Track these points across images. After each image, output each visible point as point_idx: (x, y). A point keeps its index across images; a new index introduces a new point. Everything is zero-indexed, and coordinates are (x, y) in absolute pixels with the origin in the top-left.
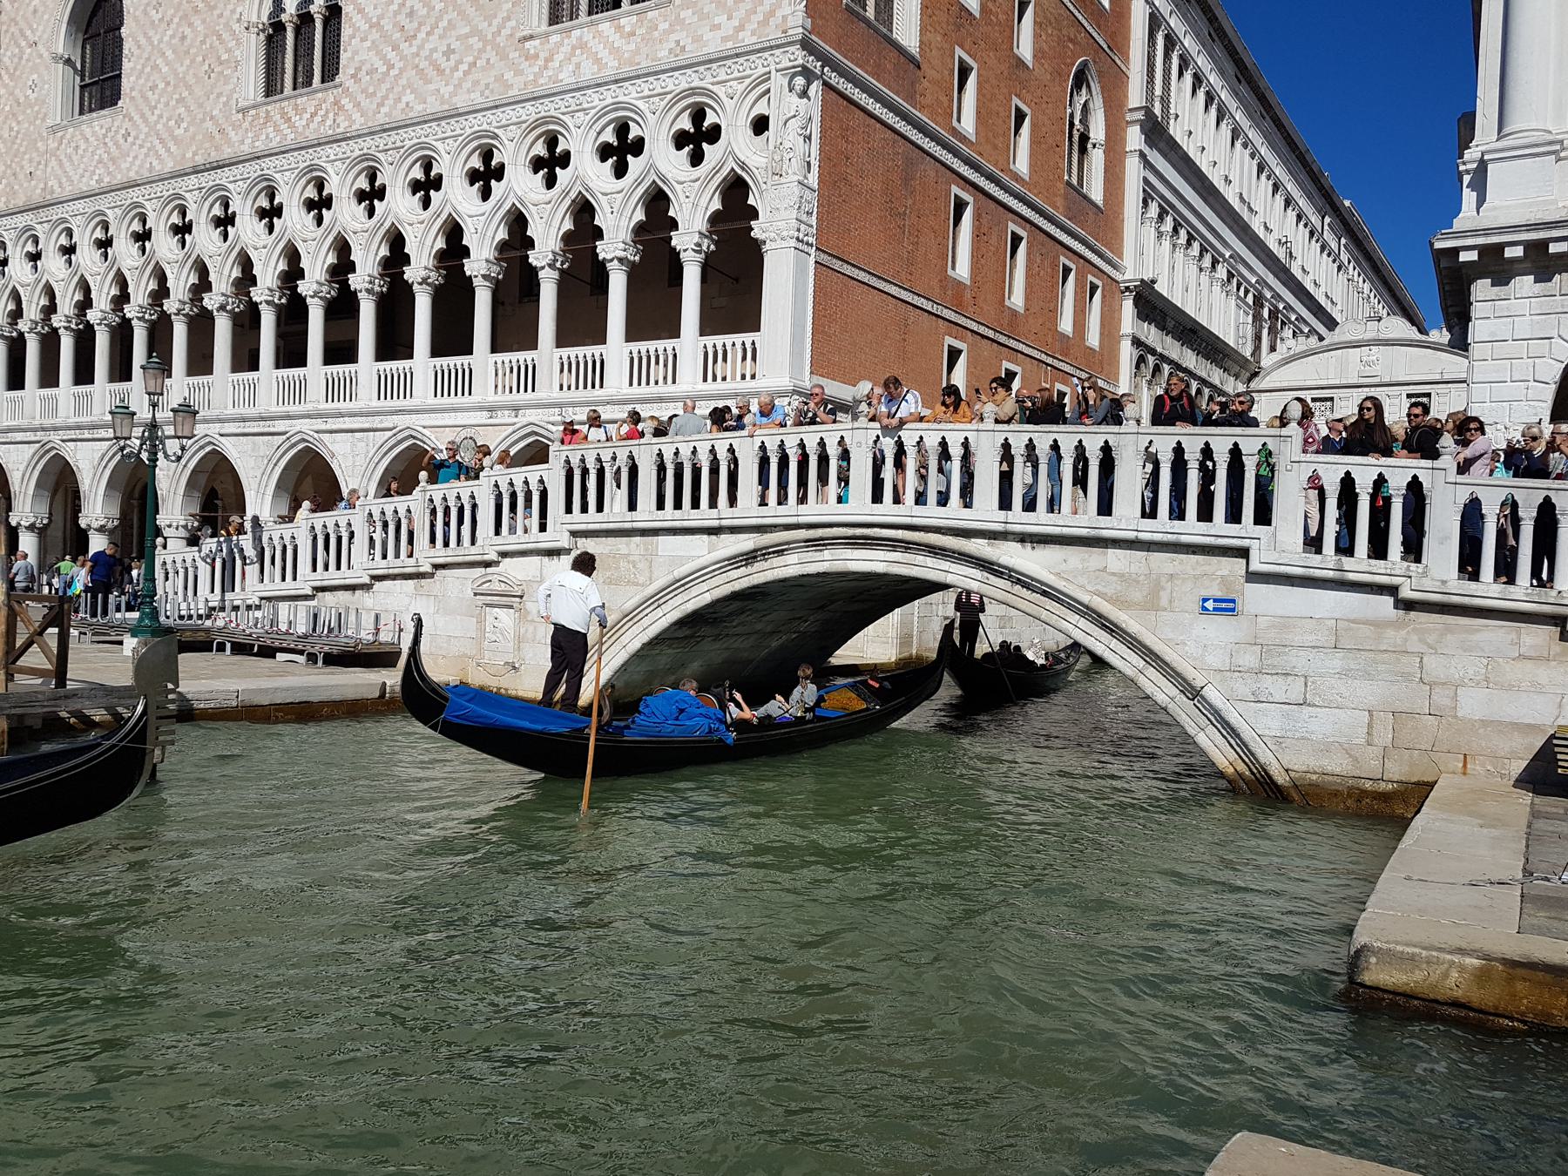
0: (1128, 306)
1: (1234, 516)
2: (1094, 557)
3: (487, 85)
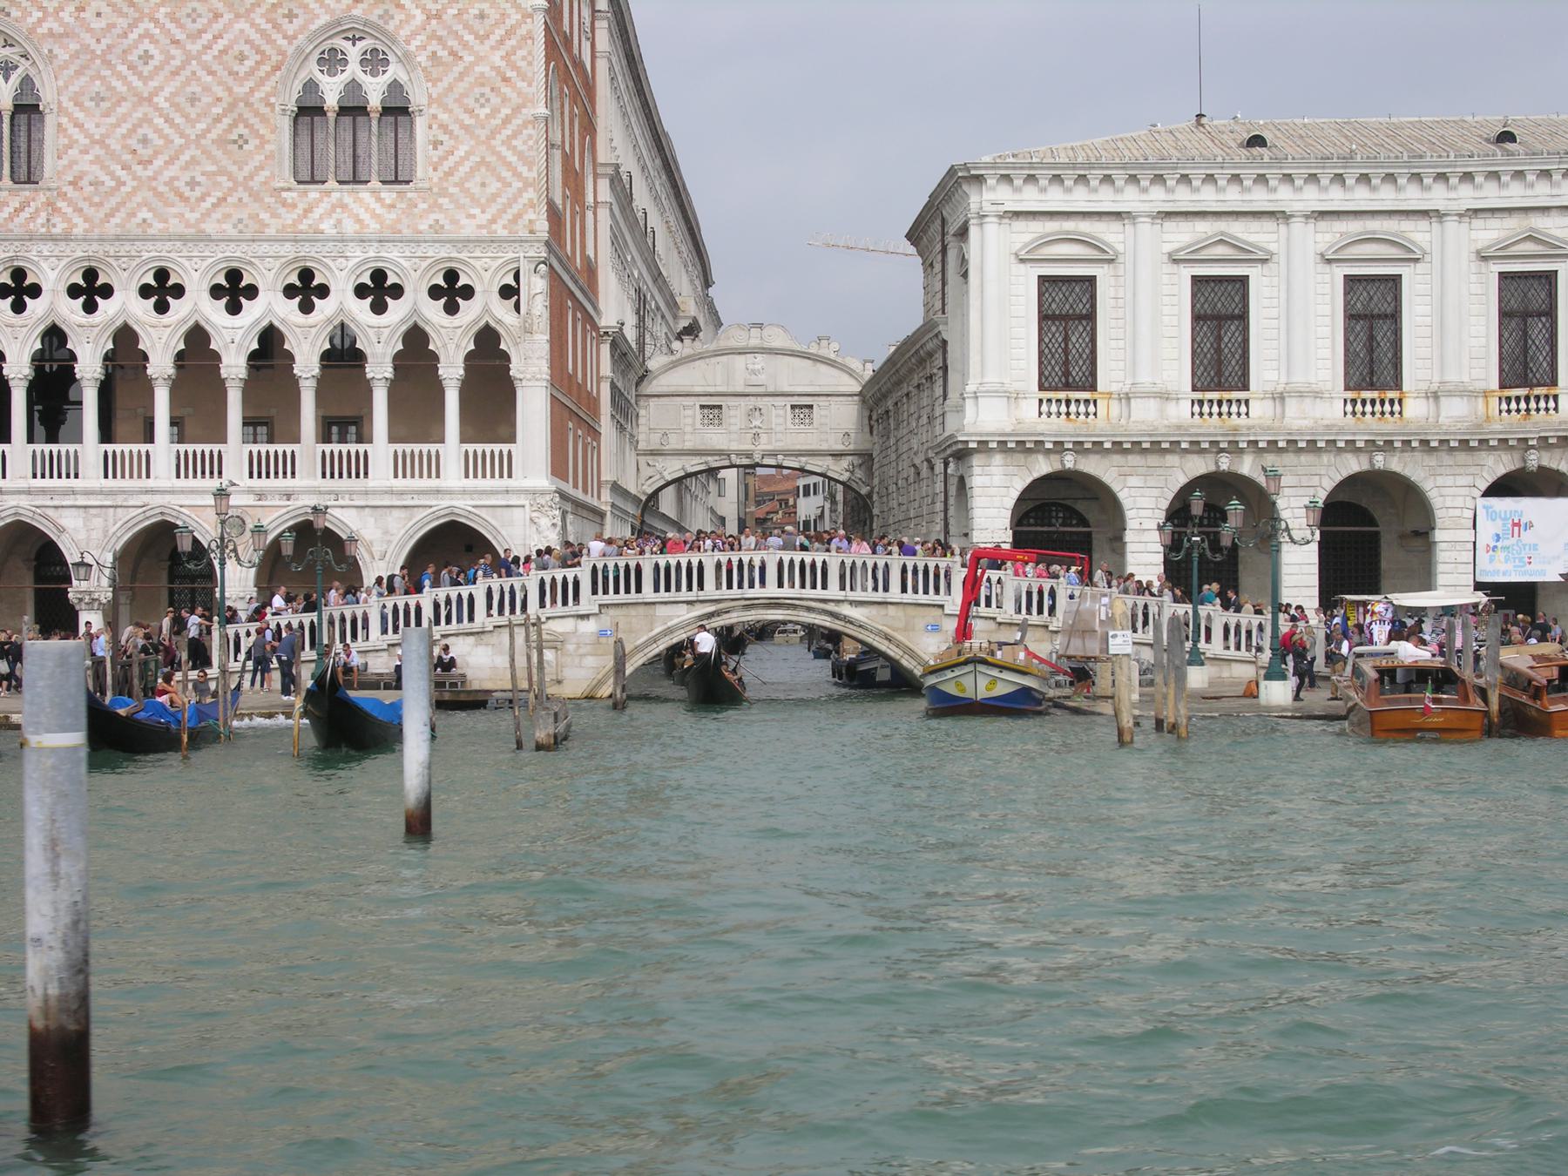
0: (605, 349)
1: (937, 591)
2: (882, 610)
3: (240, 221)
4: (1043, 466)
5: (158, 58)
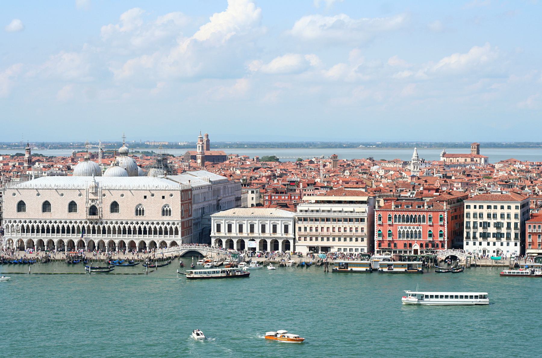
4: (217, 238)
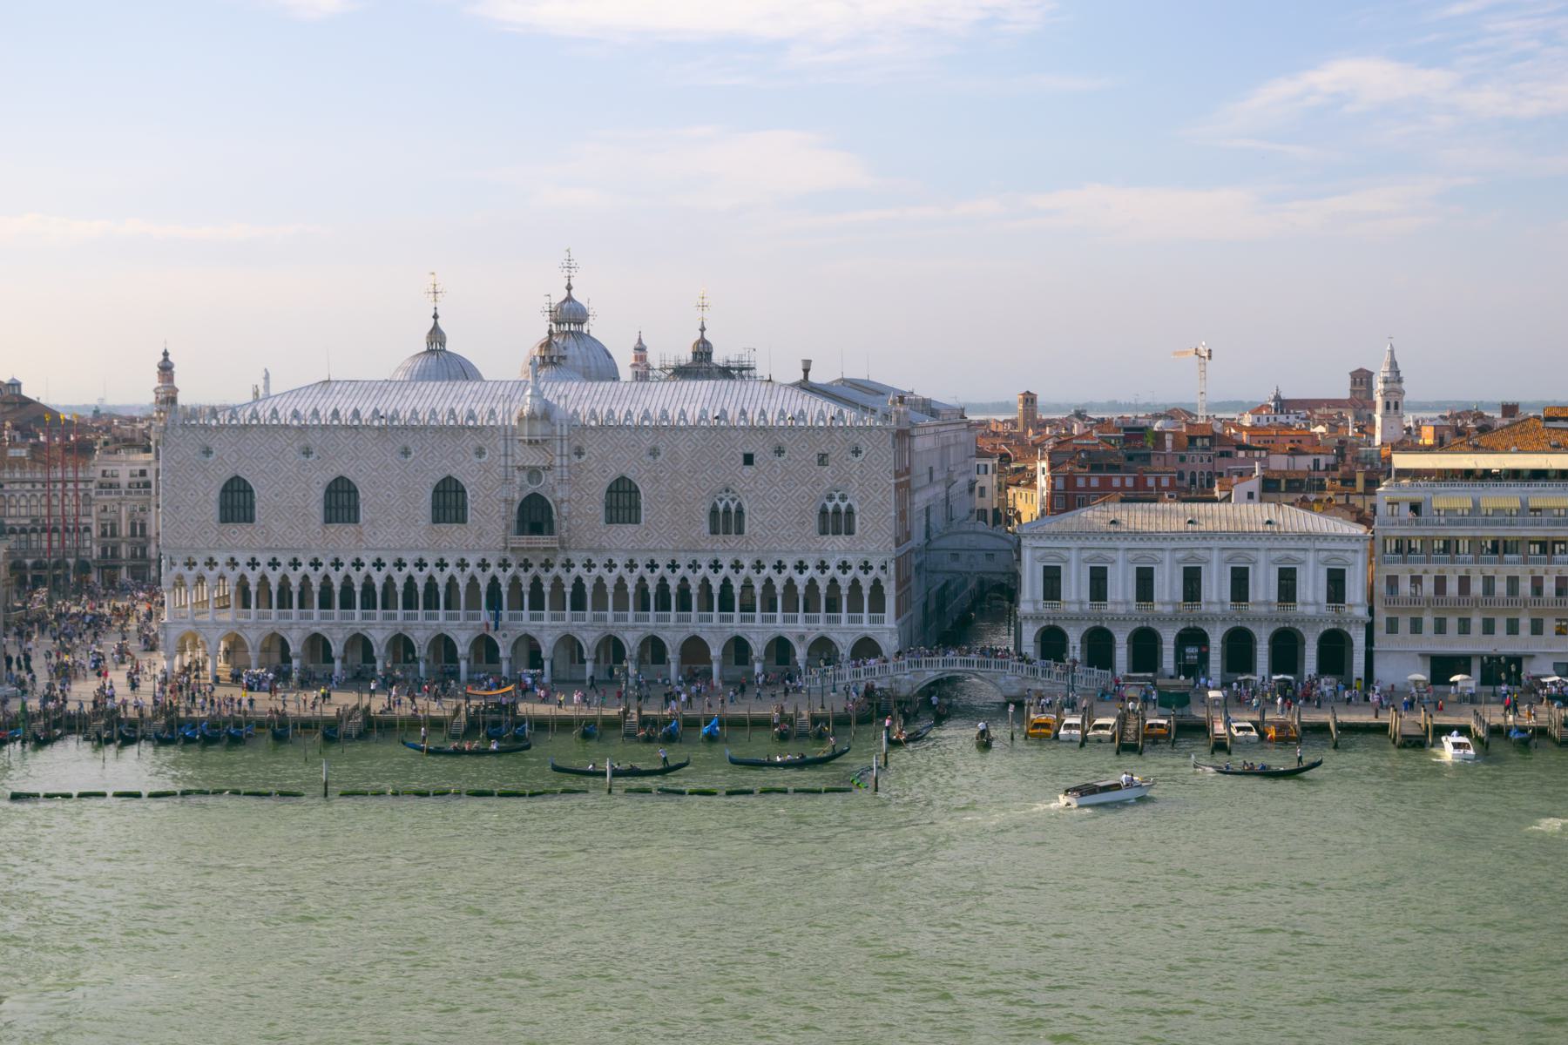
4: (1044, 624)
5: (779, 497)
